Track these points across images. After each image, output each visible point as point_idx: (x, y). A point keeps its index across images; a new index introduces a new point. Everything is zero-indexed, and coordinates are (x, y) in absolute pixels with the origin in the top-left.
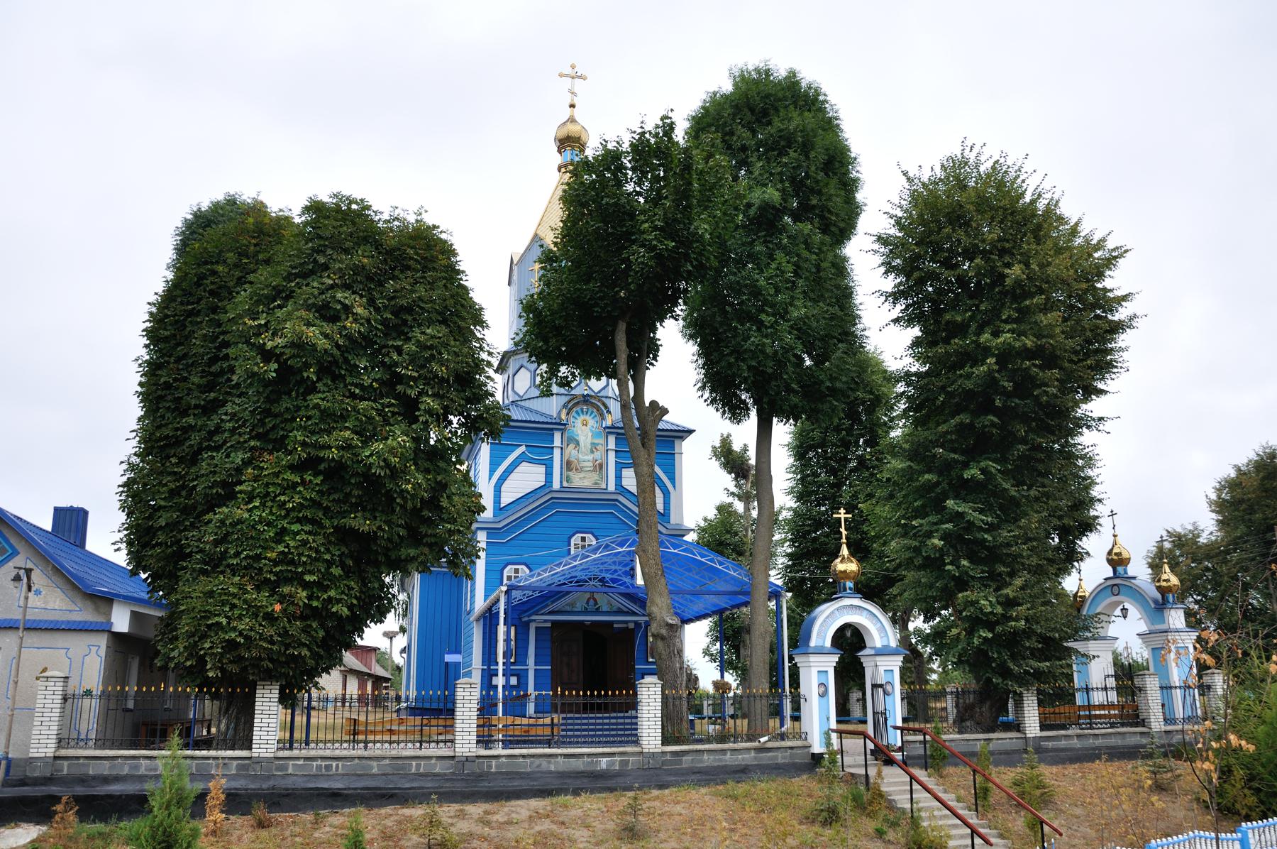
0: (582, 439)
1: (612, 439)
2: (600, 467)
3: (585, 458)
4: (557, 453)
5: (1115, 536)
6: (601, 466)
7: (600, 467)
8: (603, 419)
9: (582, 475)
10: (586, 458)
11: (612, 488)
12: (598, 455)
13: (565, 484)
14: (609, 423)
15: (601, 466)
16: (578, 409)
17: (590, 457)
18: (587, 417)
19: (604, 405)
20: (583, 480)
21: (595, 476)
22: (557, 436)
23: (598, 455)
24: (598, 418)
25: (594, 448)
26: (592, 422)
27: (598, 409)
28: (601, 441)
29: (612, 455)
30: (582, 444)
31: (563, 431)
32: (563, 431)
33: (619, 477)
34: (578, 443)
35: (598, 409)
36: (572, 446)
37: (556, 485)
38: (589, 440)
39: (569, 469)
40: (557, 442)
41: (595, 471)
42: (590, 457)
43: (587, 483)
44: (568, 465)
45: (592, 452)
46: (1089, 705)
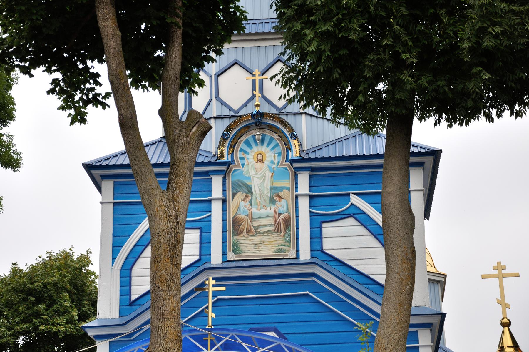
0: (256, 184)
1: (304, 179)
2: (286, 225)
3: (263, 213)
4: (216, 208)
5: (506, 325)
6: (287, 222)
7: (286, 225)
8: (289, 149)
9: (257, 239)
10: (263, 212)
11: (305, 255)
12: (282, 206)
13: (231, 256)
14: (295, 154)
15: (287, 222)
16: (248, 136)
17: (270, 210)
18: (264, 149)
19: (283, 122)
20: (258, 247)
21: (278, 240)
22: (217, 182)
23: (282, 206)
24: (281, 148)
25: (275, 195)
26: (271, 154)
27: (282, 136)
28: (288, 183)
29: (304, 204)
30: (256, 190)
31: (225, 174)
32: (225, 174)
33: (316, 237)
34: (249, 191)
35: (282, 136)
36: (240, 195)
37: (216, 259)
38: (268, 184)
39: (237, 231)
40: (217, 191)
41: (277, 230)
42: (270, 210)
43: (265, 251)
44: (235, 226)
45: (273, 201)
46: (410, 315)
